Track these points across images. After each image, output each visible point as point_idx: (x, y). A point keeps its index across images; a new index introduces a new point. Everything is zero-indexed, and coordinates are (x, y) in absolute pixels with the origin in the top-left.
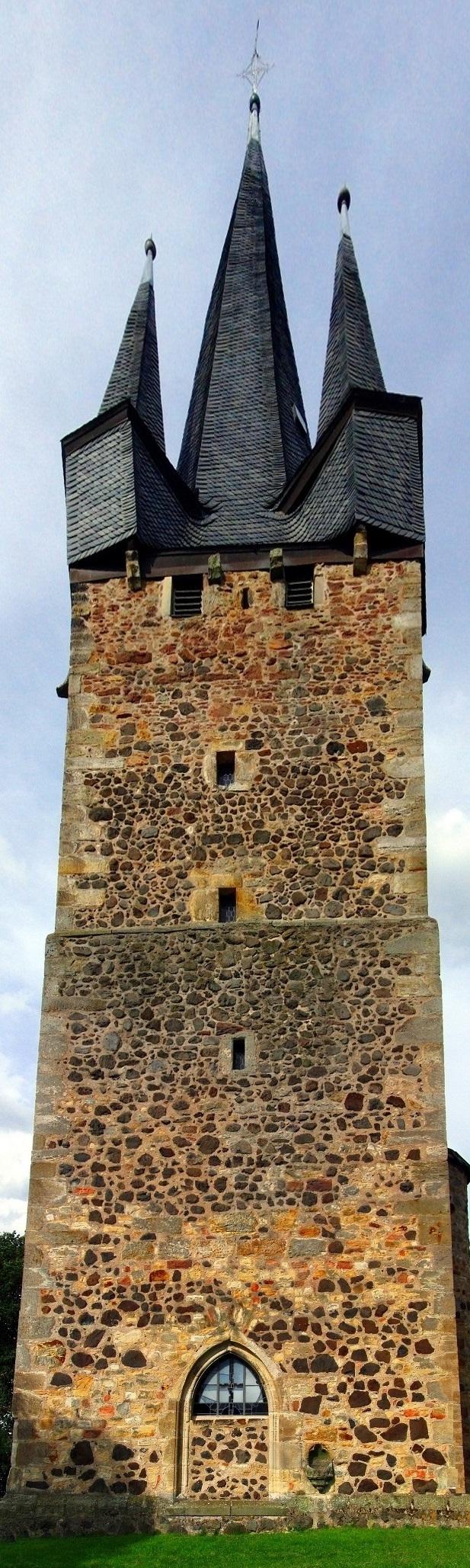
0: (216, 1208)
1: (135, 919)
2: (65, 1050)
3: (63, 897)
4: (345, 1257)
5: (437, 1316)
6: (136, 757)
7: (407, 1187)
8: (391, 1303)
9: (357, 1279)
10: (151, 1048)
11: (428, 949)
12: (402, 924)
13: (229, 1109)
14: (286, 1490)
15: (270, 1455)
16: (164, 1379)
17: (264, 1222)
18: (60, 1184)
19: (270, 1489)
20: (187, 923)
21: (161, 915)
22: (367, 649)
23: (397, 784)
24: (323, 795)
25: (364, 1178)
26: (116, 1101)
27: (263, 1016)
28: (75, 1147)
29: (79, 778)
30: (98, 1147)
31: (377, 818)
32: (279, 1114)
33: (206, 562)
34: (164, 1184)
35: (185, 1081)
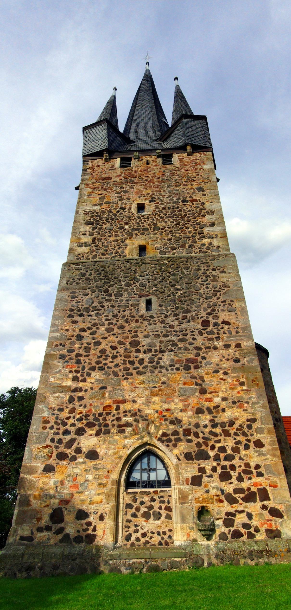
0: (139, 373)
1: (102, 257)
2: (67, 306)
3: (71, 250)
4: (208, 396)
5: (263, 426)
6: (105, 206)
7: (237, 361)
8: (237, 419)
9: (216, 407)
10: (107, 304)
11: (232, 264)
12: (219, 255)
13: (145, 328)
14: (185, 538)
15: (174, 514)
16: (109, 467)
17: (164, 379)
18: (59, 363)
19: (175, 538)
20: (125, 258)
21: (114, 255)
22: (195, 174)
23: (211, 211)
24: (181, 215)
25: (214, 357)
26: (90, 326)
27: (160, 290)
28: (68, 346)
29: (81, 212)
30: (79, 346)
31: (204, 221)
32: (169, 329)
33: (133, 154)
34: (112, 362)
35: (123, 317)
